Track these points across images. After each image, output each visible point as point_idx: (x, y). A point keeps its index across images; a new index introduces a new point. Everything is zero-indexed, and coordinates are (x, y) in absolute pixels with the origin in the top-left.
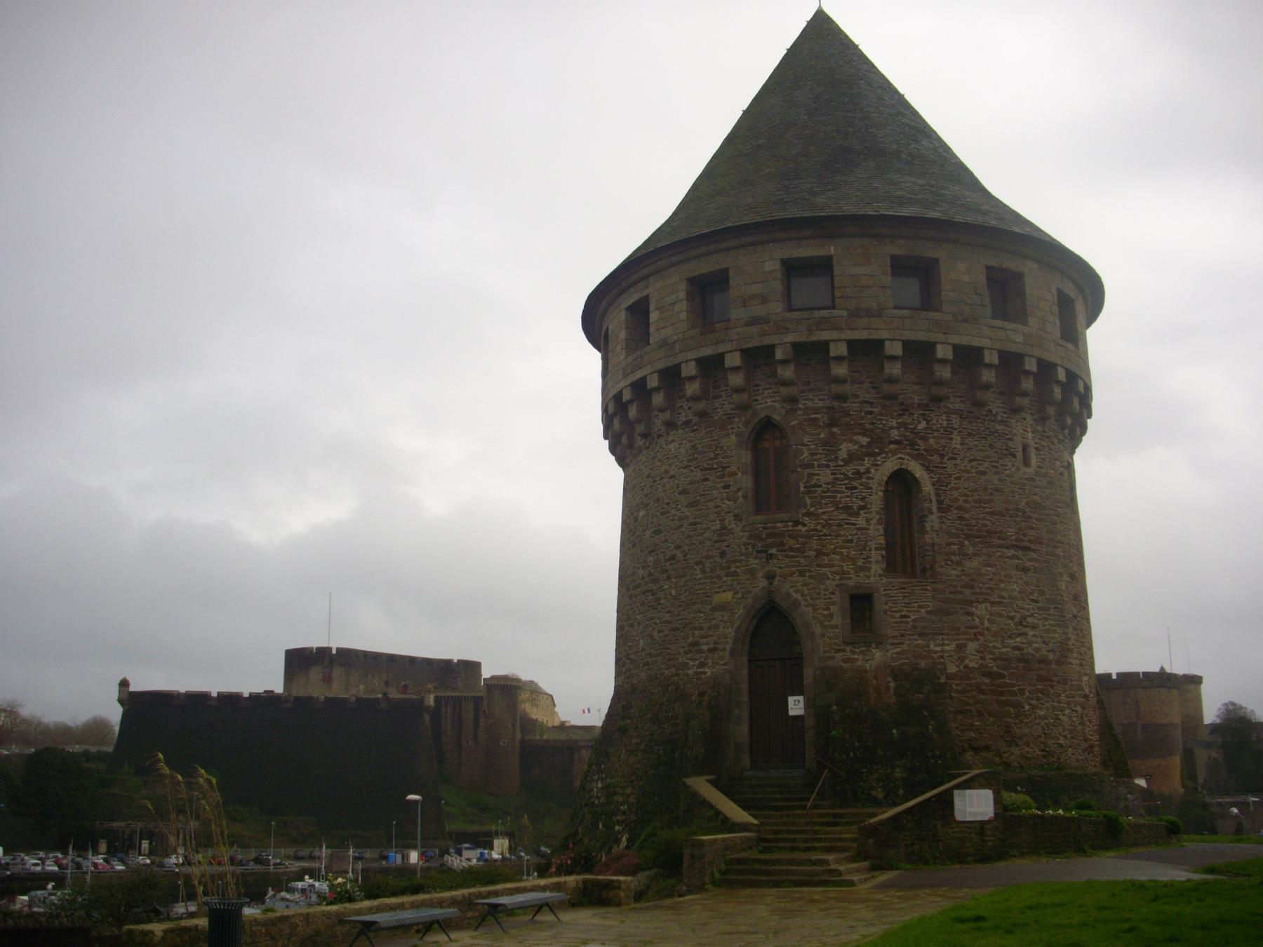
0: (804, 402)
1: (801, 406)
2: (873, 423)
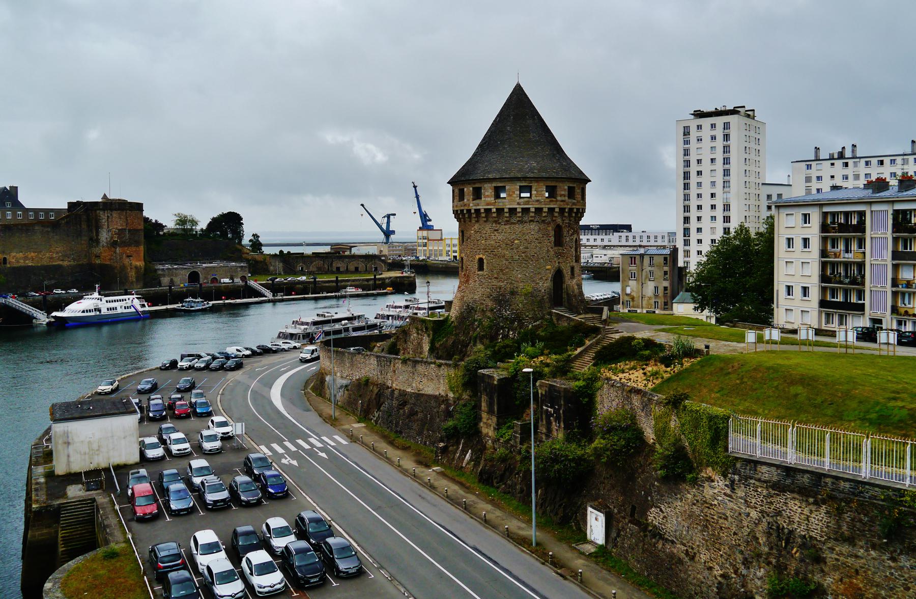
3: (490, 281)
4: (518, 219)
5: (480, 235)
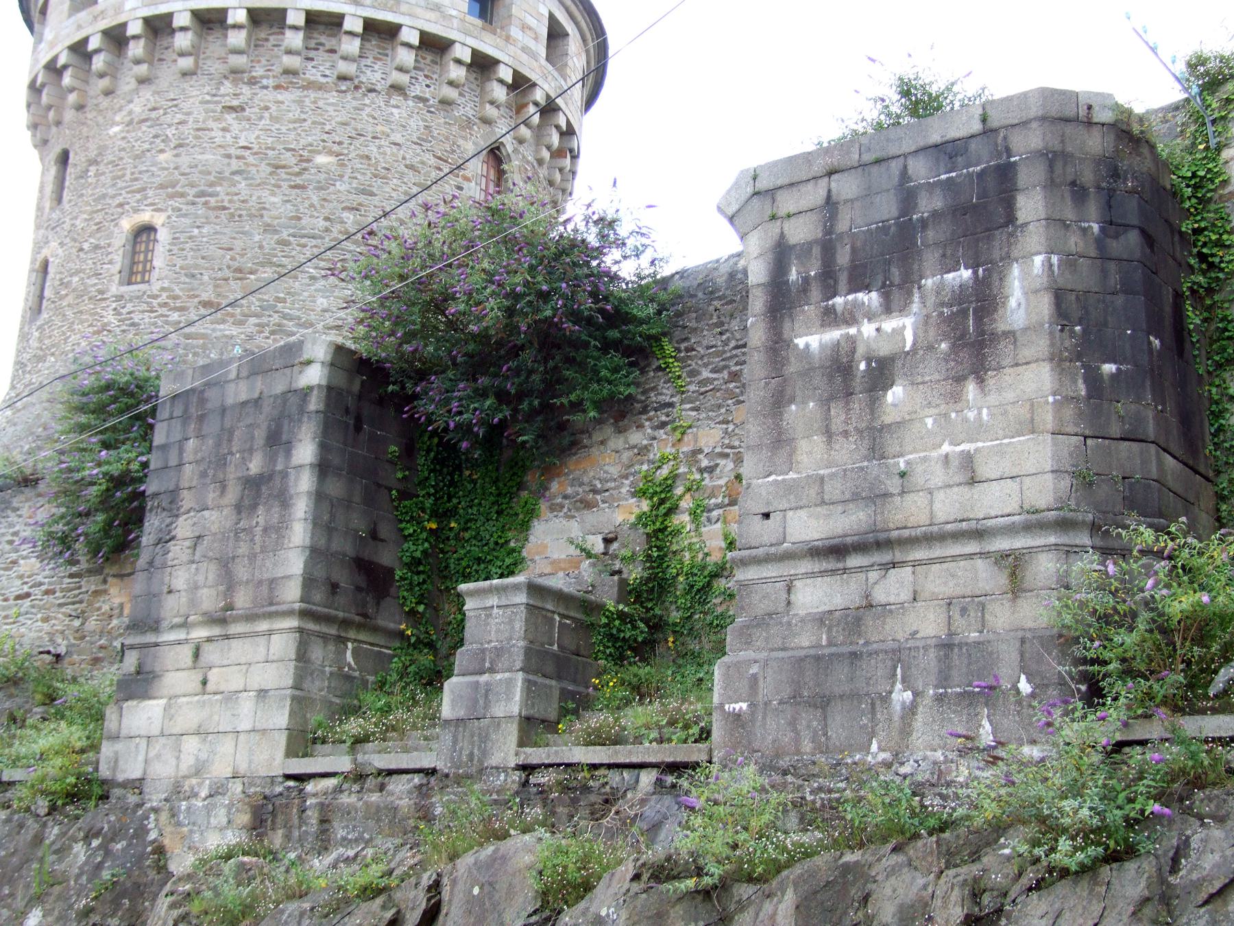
3: (175, 316)
4: (344, 67)
5: (153, 131)
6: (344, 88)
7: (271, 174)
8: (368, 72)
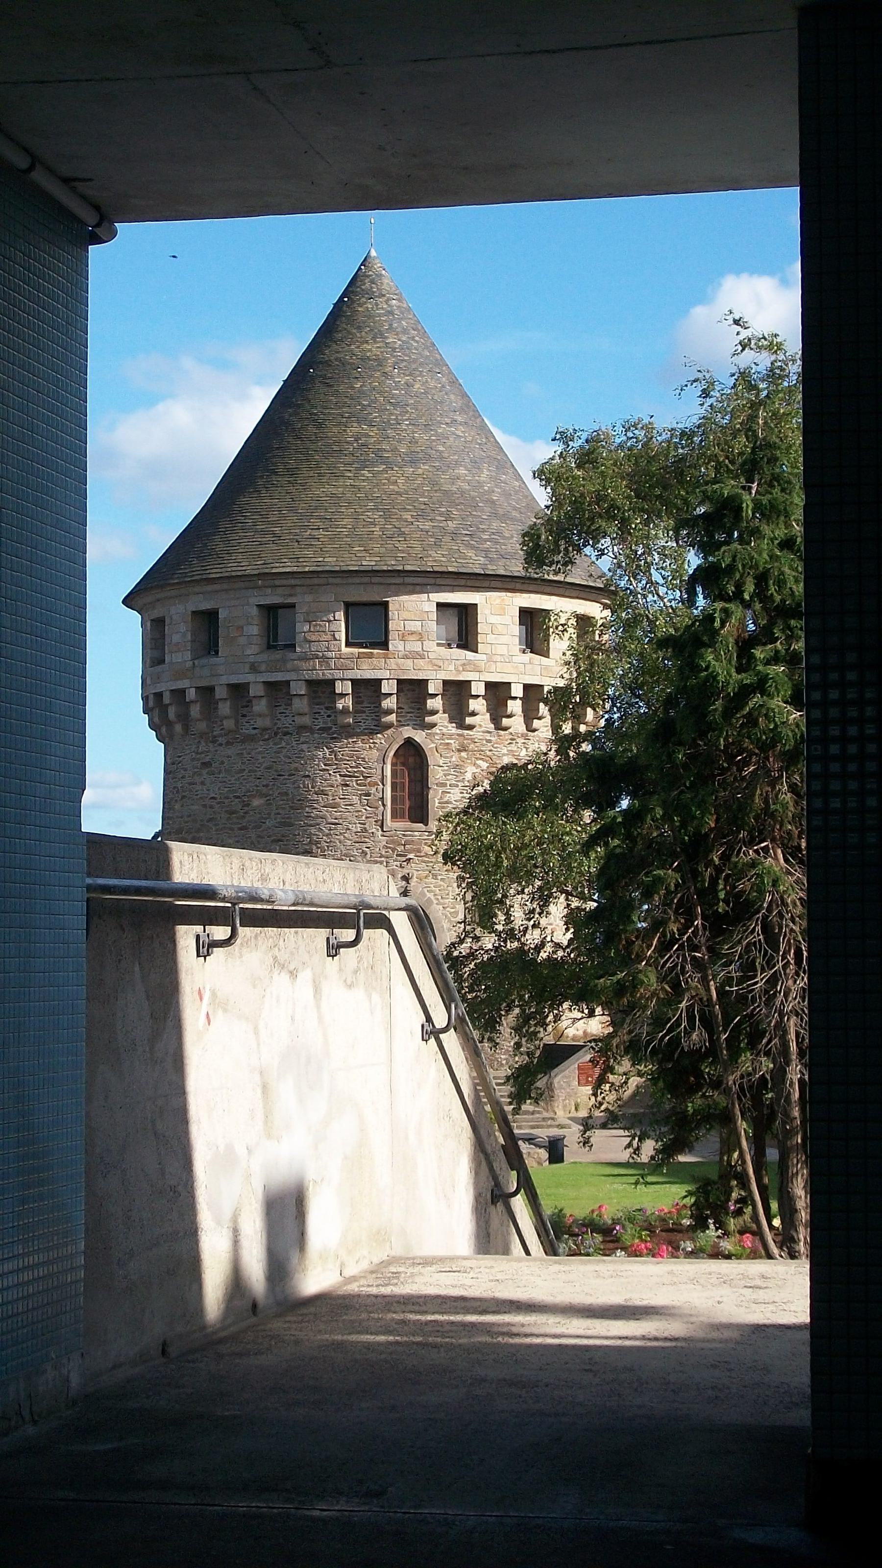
0: (441, 728)
1: (438, 731)
2: (490, 751)
6: (267, 737)
7: (229, 819)
8: (283, 718)
